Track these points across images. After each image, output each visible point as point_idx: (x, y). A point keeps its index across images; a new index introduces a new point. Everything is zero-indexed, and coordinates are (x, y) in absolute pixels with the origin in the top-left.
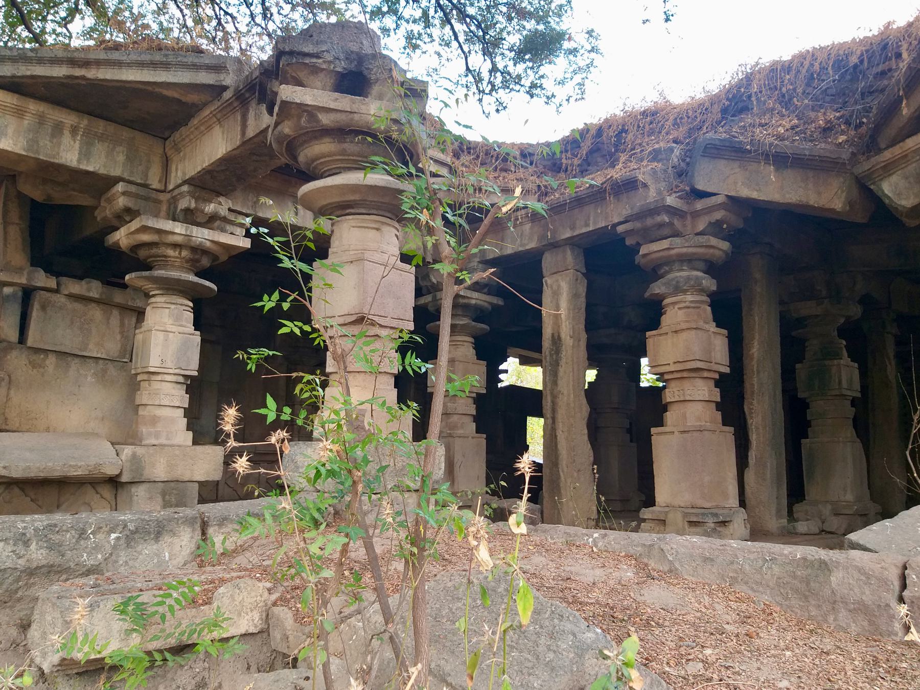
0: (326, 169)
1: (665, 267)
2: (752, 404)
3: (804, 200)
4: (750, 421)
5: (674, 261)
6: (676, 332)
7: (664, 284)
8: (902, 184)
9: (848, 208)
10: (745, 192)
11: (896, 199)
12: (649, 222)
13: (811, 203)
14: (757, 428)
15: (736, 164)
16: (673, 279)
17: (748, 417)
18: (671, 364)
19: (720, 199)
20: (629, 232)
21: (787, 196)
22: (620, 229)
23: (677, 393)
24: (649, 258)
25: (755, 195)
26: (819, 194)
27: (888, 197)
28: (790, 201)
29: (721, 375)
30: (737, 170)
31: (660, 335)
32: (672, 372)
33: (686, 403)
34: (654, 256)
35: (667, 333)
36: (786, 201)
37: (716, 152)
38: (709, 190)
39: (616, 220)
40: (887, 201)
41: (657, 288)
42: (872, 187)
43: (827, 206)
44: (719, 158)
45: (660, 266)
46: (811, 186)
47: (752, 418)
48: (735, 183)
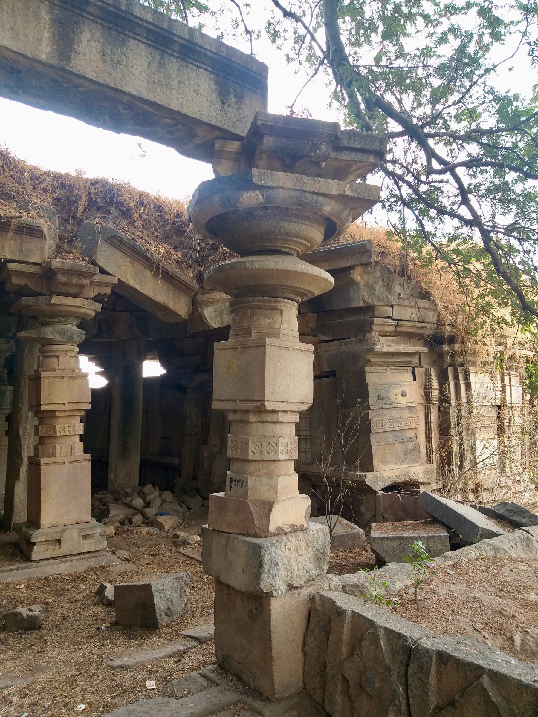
0: (292, 247)
1: (60, 318)
2: (25, 428)
3: (167, 304)
4: (23, 442)
5: (70, 316)
6: (71, 377)
7: (60, 333)
8: (213, 314)
9: (187, 317)
10: (132, 283)
11: (209, 321)
12: (75, 280)
13: (170, 307)
14: (28, 447)
15: (129, 259)
16: (68, 331)
17: (22, 439)
18: (66, 404)
19: (115, 281)
20: (19, 273)
21: (158, 296)
22: (12, 266)
23: (67, 428)
24: (56, 307)
25: (138, 287)
26: (175, 302)
27: (206, 319)
28: (159, 301)
29: (87, 411)
30: (128, 264)
31: (55, 377)
32: (65, 411)
33: (72, 437)
34: (65, 308)
35: (63, 377)
36: (156, 300)
37: (118, 243)
38: (107, 269)
39: (9, 256)
40: (205, 321)
41: (49, 333)
42: (199, 309)
43: (177, 312)
44: (118, 249)
45: (57, 316)
46: (171, 295)
47: (25, 439)
48: (126, 273)
